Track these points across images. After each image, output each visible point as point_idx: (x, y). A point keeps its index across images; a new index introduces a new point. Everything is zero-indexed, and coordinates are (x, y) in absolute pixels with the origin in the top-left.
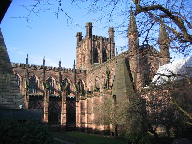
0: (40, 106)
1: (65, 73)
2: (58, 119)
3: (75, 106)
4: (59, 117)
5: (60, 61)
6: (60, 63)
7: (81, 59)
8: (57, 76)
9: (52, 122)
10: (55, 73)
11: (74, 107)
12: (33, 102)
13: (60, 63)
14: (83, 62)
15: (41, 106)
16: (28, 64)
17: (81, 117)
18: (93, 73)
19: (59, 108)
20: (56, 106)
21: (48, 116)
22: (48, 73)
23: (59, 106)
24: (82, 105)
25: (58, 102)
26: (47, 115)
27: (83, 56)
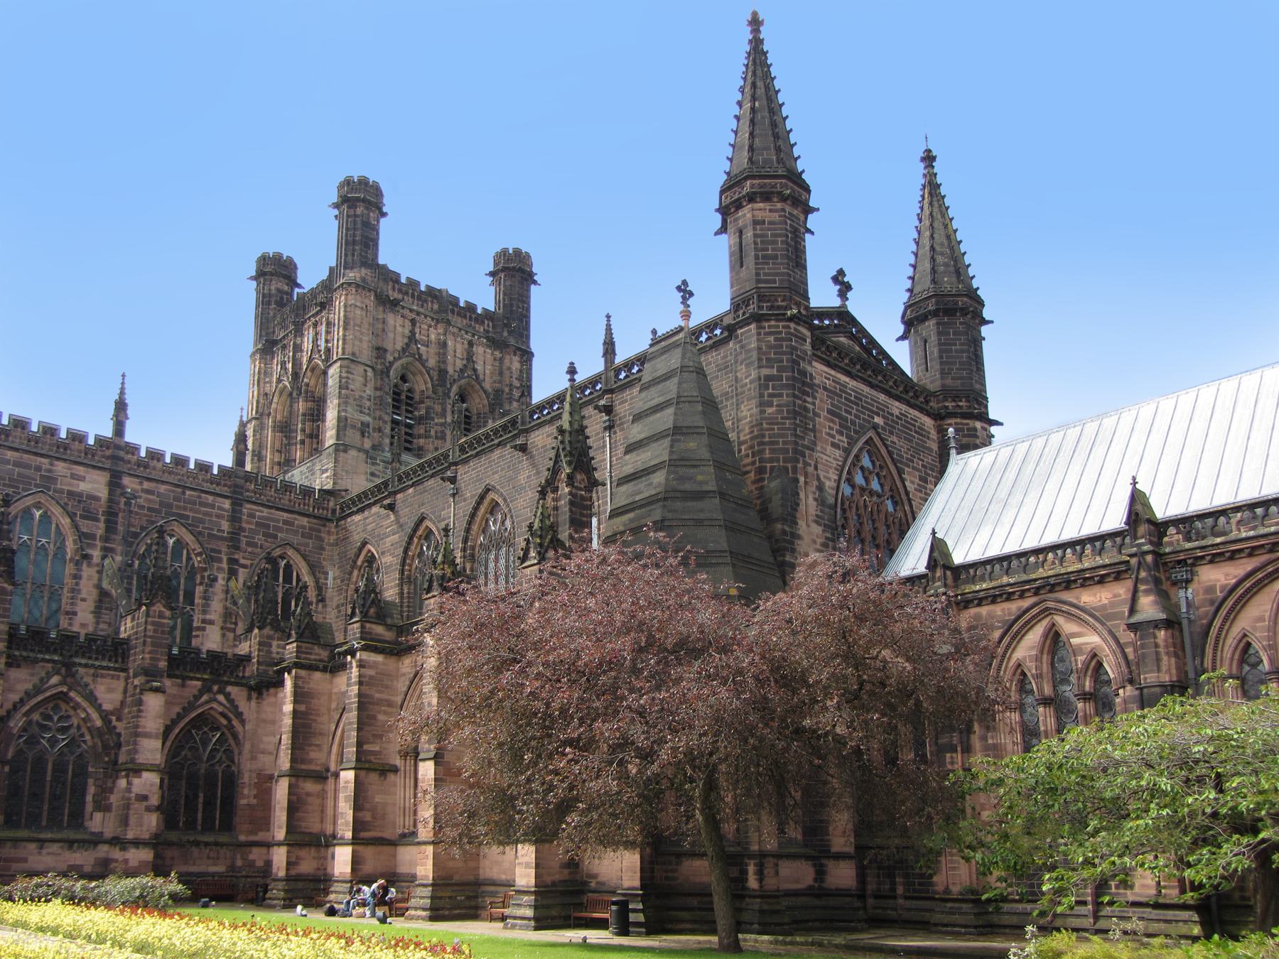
7: (285, 428)
14: (303, 442)
18: (391, 507)
19: (99, 723)
20: (77, 707)
23: (99, 708)
27: (301, 406)
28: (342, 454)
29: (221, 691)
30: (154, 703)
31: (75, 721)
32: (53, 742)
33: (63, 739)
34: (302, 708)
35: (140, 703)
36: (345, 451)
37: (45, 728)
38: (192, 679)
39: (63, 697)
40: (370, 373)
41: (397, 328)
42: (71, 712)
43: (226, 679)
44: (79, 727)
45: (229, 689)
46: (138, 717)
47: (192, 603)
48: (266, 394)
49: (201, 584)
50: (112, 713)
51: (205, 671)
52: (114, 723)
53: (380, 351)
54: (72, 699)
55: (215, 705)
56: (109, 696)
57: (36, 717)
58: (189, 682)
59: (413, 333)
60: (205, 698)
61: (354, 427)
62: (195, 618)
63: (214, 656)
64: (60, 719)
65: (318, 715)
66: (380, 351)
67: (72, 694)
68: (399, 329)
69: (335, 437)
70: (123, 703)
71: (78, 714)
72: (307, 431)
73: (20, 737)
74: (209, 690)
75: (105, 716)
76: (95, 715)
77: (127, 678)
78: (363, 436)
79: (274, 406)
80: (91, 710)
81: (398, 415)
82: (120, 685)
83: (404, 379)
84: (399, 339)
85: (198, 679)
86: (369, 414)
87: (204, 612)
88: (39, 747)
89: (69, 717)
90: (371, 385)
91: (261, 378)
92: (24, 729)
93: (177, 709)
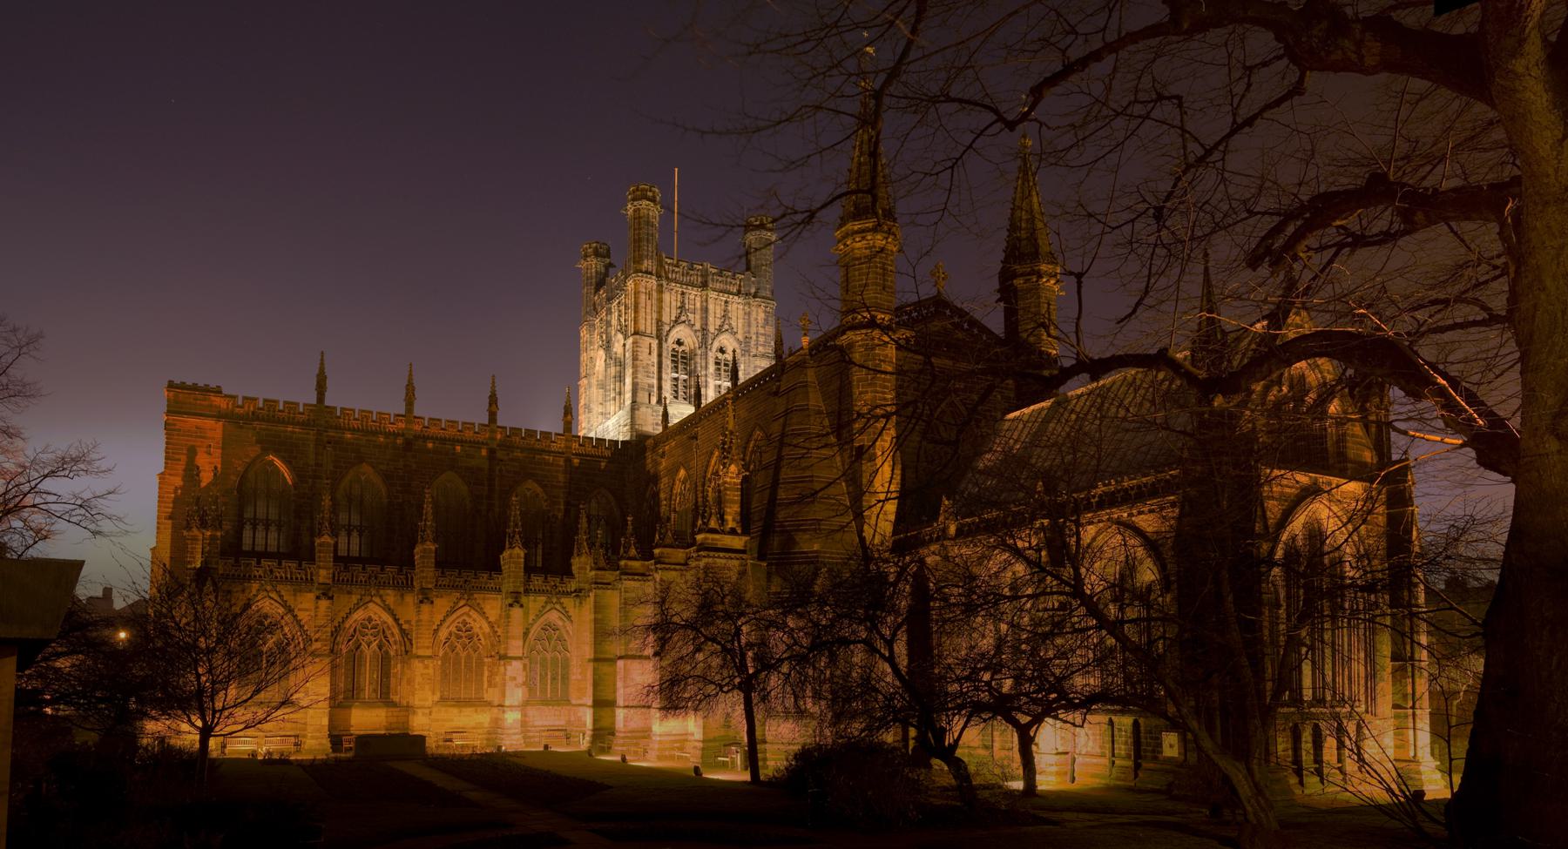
4: (486, 673)
6: (493, 400)
13: (493, 400)
17: (594, 674)
19: (487, 629)
24: (599, 616)
25: (484, 599)
27: (613, 370)
34: (599, 616)
35: (508, 617)
37: (459, 637)
45: (562, 600)
52: (496, 629)
57: (454, 630)
59: (683, 302)
60: (548, 608)
68: (674, 304)
70: (500, 615)
72: (617, 390)
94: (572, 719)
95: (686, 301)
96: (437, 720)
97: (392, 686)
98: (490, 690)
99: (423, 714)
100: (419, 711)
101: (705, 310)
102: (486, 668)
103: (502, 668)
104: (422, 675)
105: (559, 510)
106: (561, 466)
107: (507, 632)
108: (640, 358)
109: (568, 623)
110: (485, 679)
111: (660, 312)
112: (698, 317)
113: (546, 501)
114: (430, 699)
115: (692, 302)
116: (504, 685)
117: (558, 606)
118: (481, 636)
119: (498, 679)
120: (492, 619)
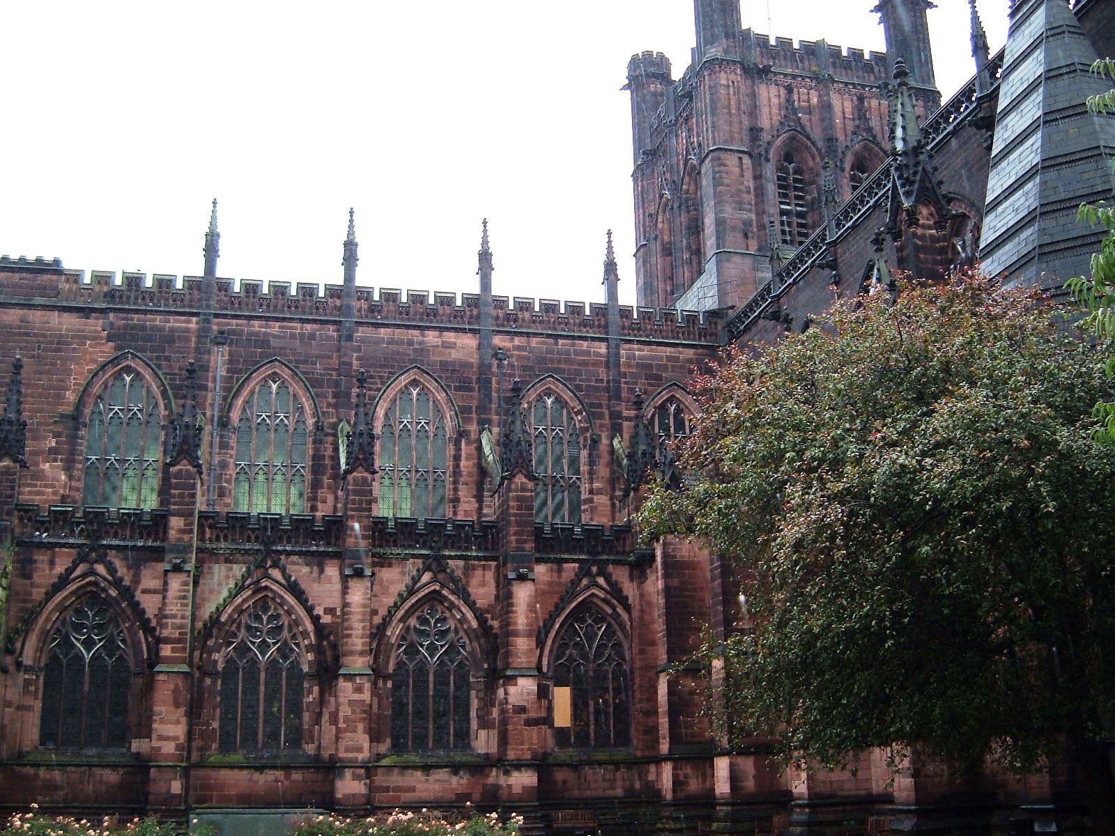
0: (301, 611)
1: (534, 342)
2: (474, 724)
3: (620, 610)
4: (475, 703)
5: (485, 242)
6: (485, 258)
8: (470, 365)
9: (414, 758)
10: (446, 345)
11: (616, 616)
12: (239, 570)
13: (485, 258)
15: (309, 610)
16: (218, 274)
19: (474, 624)
20: (452, 606)
21: (366, 696)
22: (391, 342)
23: (472, 605)
26: (359, 690)
28: (726, 264)
29: (601, 573)
30: (523, 594)
31: (451, 624)
32: (432, 649)
33: (442, 646)
34: (675, 582)
35: (509, 595)
36: (728, 261)
38: (567, 561)
39: (435, 597)
40: (747, 161)
41: (770, 97)
42: (448, 614)
43: (605, 557)
44: (456, 631)
46: (508, 612)
47: (577, 472)
48: (650, 215)
49: (585, 447)
50: (487, 611)
51: (582, 552)
52: (490, 622)
53: (755, 132)
54: (446, 598)
55: (595, 591)
56: (481, 591)
57: (413, 622)
58: (565, 565)
60: (585, 582)
61: (733, 228)
62: (582, 489)
63: (593, 534)
64: (437, 621)
65: (695, 590)
66: (755, 132)
67: (445, 592)
69: (715, 246)
71: (454, 616)
72: (694, 247)
73: (400, 646)
74: (588, 574)
75: (479, 615)
76: (470, 615)
77: (498, 567)
78: (746, 236)
79: (660, 225)
80: (465, 609)
81: (788, 204)
82: (490, 576)
83: (788, 158)
84: (775, 111)
85: (574, 561)
86: (750, 211)
87: (591, 481)
88: (418, 657)
89: (445, 619)
90: (749, 174)
91: (641, 199)
92: (403, 638)
93: (555, 599)
94: (637, 785)
95: (795, 97)
96: (387, 789)
97: (306, 727)
98: (483, 733)
99: (356, 777)
100: (348, 773)
101: (827, 107)
102: (473, 693)
103: (501, 692)
104: (350, 703)
105: (601, 426)
106: (599, 355)
107: (508, 624)
108: (726, 181)
109: (620, 610)
110: (473, 714)
111: (754, 111)
112: (815, 118)
113: (580, 412)
114: (366, 745)
115: (804, 97)
116: (504, 722)
117: (601, 581)
118: (461, 633)
119: (495, 713)
120: (481, 603)
